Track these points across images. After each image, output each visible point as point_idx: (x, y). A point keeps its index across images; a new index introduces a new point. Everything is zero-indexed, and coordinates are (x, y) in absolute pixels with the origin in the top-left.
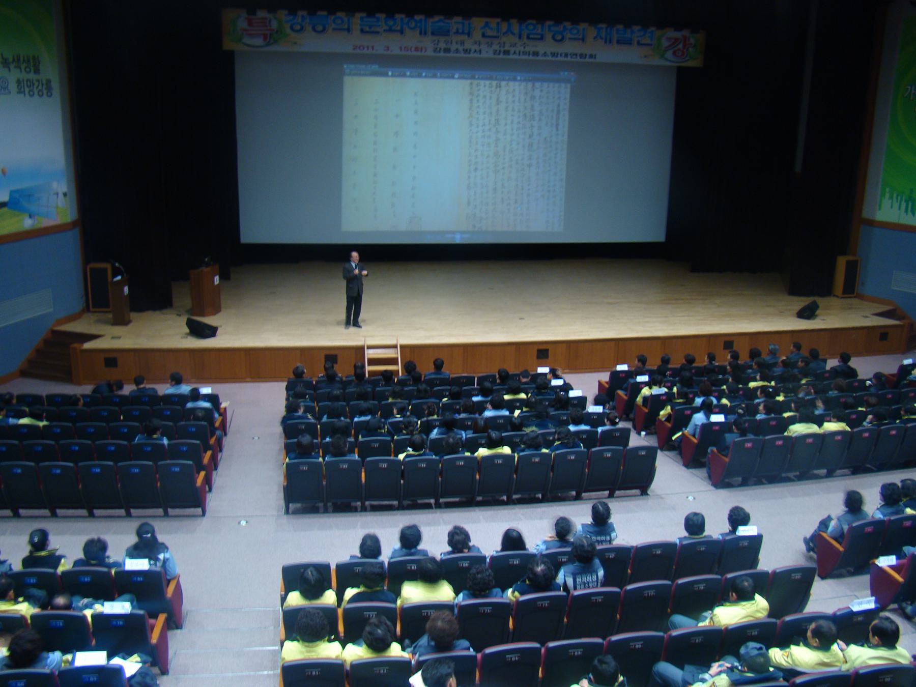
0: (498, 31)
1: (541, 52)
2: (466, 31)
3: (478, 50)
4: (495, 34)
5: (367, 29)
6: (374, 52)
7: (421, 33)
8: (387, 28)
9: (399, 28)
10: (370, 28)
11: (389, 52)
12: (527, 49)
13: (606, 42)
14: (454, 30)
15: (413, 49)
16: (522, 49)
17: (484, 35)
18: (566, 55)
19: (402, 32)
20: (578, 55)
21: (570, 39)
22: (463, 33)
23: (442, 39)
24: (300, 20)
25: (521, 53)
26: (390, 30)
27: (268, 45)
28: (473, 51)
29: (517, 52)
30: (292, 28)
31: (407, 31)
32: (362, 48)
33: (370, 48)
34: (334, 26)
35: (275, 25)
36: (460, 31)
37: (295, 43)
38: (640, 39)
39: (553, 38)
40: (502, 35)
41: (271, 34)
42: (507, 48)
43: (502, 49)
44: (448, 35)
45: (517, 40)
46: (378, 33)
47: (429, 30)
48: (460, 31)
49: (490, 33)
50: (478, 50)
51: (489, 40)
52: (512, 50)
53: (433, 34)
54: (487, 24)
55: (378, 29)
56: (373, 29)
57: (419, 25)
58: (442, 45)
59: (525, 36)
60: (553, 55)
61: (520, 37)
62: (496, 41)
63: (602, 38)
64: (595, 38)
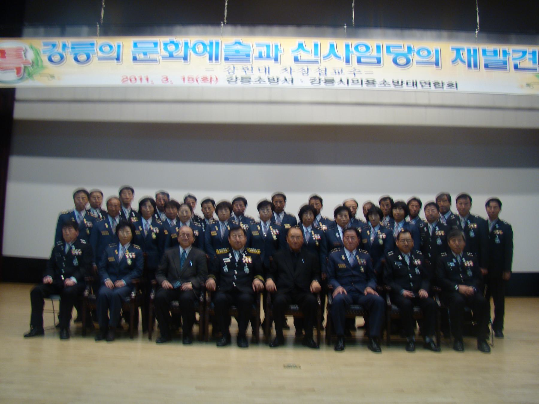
0: (316, 54)
1: (378, 80)
2: (272, 55)
3: (289, 78)
4: (313, 58)
5: (142, 57)
6: (150, 83)
7: (211, 59)
8: (167, 54)
9: (182, 54)
10: (145, 54)
11: (169, 84)
12: (358, 77)
13: (469, 66)
14: (257, 55)
15: (200, 80)
16: (351, 77)
17: (296, 60)
18: (415, 84)
19: (185, 58)
20: (432, 84)
21: (418, 63)
22: (268, 57)
23: (239, 66)
24: (60, 50)
25: (350, 81)
26: (171, 56)
27: (21, 79)
28: (282, 79)
29: (345, 81)
30: (50, 60)
31: (192, 55)
32: (133, 80)
33: (144, 81)
34: (100, 54)
35: (31, 56)
36: (264, 55)
37: (52, 77)
38: (517, 62)
39: (395, 62)
40: (322, 58)
41: (25, 67)
42: (329, 76)
43: (323, 78)
44: (249, 61)
45: (342, 64)
46: (155, 61)
47: (222, 56)
48: (264, 55)
49: (303, 56)
50: (289, 78)
51: (305, 66)
52: (337, 79)
53: (227, 59)
54: (301, 46)
55: (153, 56)
56: (148, 57)
57: (208, 49)
58: (240, 74)
59: (355, 60)
60: (396, 83)
61: (348, 61)
62: (313, 68)
63: (464, 62)
64: (454, 61)
